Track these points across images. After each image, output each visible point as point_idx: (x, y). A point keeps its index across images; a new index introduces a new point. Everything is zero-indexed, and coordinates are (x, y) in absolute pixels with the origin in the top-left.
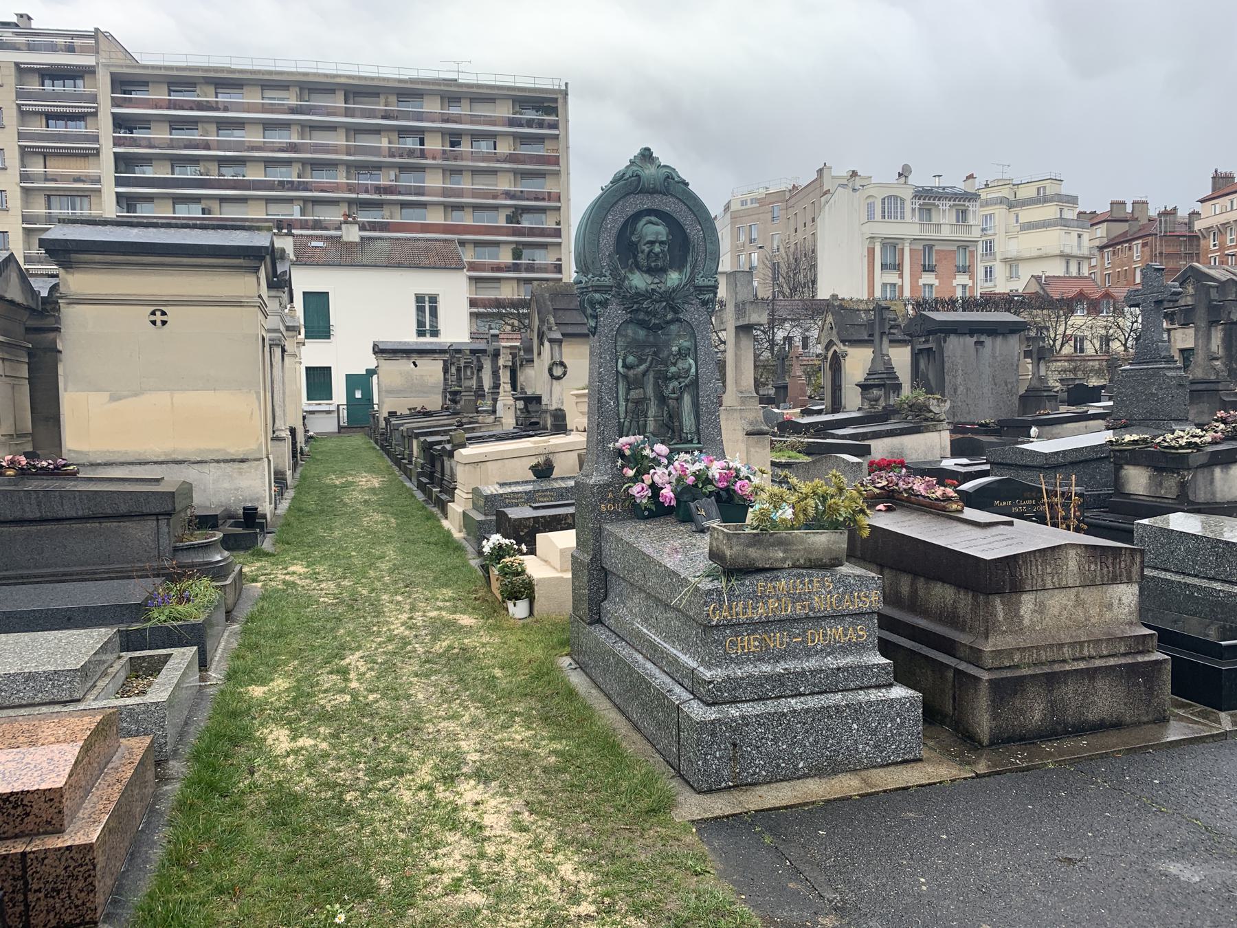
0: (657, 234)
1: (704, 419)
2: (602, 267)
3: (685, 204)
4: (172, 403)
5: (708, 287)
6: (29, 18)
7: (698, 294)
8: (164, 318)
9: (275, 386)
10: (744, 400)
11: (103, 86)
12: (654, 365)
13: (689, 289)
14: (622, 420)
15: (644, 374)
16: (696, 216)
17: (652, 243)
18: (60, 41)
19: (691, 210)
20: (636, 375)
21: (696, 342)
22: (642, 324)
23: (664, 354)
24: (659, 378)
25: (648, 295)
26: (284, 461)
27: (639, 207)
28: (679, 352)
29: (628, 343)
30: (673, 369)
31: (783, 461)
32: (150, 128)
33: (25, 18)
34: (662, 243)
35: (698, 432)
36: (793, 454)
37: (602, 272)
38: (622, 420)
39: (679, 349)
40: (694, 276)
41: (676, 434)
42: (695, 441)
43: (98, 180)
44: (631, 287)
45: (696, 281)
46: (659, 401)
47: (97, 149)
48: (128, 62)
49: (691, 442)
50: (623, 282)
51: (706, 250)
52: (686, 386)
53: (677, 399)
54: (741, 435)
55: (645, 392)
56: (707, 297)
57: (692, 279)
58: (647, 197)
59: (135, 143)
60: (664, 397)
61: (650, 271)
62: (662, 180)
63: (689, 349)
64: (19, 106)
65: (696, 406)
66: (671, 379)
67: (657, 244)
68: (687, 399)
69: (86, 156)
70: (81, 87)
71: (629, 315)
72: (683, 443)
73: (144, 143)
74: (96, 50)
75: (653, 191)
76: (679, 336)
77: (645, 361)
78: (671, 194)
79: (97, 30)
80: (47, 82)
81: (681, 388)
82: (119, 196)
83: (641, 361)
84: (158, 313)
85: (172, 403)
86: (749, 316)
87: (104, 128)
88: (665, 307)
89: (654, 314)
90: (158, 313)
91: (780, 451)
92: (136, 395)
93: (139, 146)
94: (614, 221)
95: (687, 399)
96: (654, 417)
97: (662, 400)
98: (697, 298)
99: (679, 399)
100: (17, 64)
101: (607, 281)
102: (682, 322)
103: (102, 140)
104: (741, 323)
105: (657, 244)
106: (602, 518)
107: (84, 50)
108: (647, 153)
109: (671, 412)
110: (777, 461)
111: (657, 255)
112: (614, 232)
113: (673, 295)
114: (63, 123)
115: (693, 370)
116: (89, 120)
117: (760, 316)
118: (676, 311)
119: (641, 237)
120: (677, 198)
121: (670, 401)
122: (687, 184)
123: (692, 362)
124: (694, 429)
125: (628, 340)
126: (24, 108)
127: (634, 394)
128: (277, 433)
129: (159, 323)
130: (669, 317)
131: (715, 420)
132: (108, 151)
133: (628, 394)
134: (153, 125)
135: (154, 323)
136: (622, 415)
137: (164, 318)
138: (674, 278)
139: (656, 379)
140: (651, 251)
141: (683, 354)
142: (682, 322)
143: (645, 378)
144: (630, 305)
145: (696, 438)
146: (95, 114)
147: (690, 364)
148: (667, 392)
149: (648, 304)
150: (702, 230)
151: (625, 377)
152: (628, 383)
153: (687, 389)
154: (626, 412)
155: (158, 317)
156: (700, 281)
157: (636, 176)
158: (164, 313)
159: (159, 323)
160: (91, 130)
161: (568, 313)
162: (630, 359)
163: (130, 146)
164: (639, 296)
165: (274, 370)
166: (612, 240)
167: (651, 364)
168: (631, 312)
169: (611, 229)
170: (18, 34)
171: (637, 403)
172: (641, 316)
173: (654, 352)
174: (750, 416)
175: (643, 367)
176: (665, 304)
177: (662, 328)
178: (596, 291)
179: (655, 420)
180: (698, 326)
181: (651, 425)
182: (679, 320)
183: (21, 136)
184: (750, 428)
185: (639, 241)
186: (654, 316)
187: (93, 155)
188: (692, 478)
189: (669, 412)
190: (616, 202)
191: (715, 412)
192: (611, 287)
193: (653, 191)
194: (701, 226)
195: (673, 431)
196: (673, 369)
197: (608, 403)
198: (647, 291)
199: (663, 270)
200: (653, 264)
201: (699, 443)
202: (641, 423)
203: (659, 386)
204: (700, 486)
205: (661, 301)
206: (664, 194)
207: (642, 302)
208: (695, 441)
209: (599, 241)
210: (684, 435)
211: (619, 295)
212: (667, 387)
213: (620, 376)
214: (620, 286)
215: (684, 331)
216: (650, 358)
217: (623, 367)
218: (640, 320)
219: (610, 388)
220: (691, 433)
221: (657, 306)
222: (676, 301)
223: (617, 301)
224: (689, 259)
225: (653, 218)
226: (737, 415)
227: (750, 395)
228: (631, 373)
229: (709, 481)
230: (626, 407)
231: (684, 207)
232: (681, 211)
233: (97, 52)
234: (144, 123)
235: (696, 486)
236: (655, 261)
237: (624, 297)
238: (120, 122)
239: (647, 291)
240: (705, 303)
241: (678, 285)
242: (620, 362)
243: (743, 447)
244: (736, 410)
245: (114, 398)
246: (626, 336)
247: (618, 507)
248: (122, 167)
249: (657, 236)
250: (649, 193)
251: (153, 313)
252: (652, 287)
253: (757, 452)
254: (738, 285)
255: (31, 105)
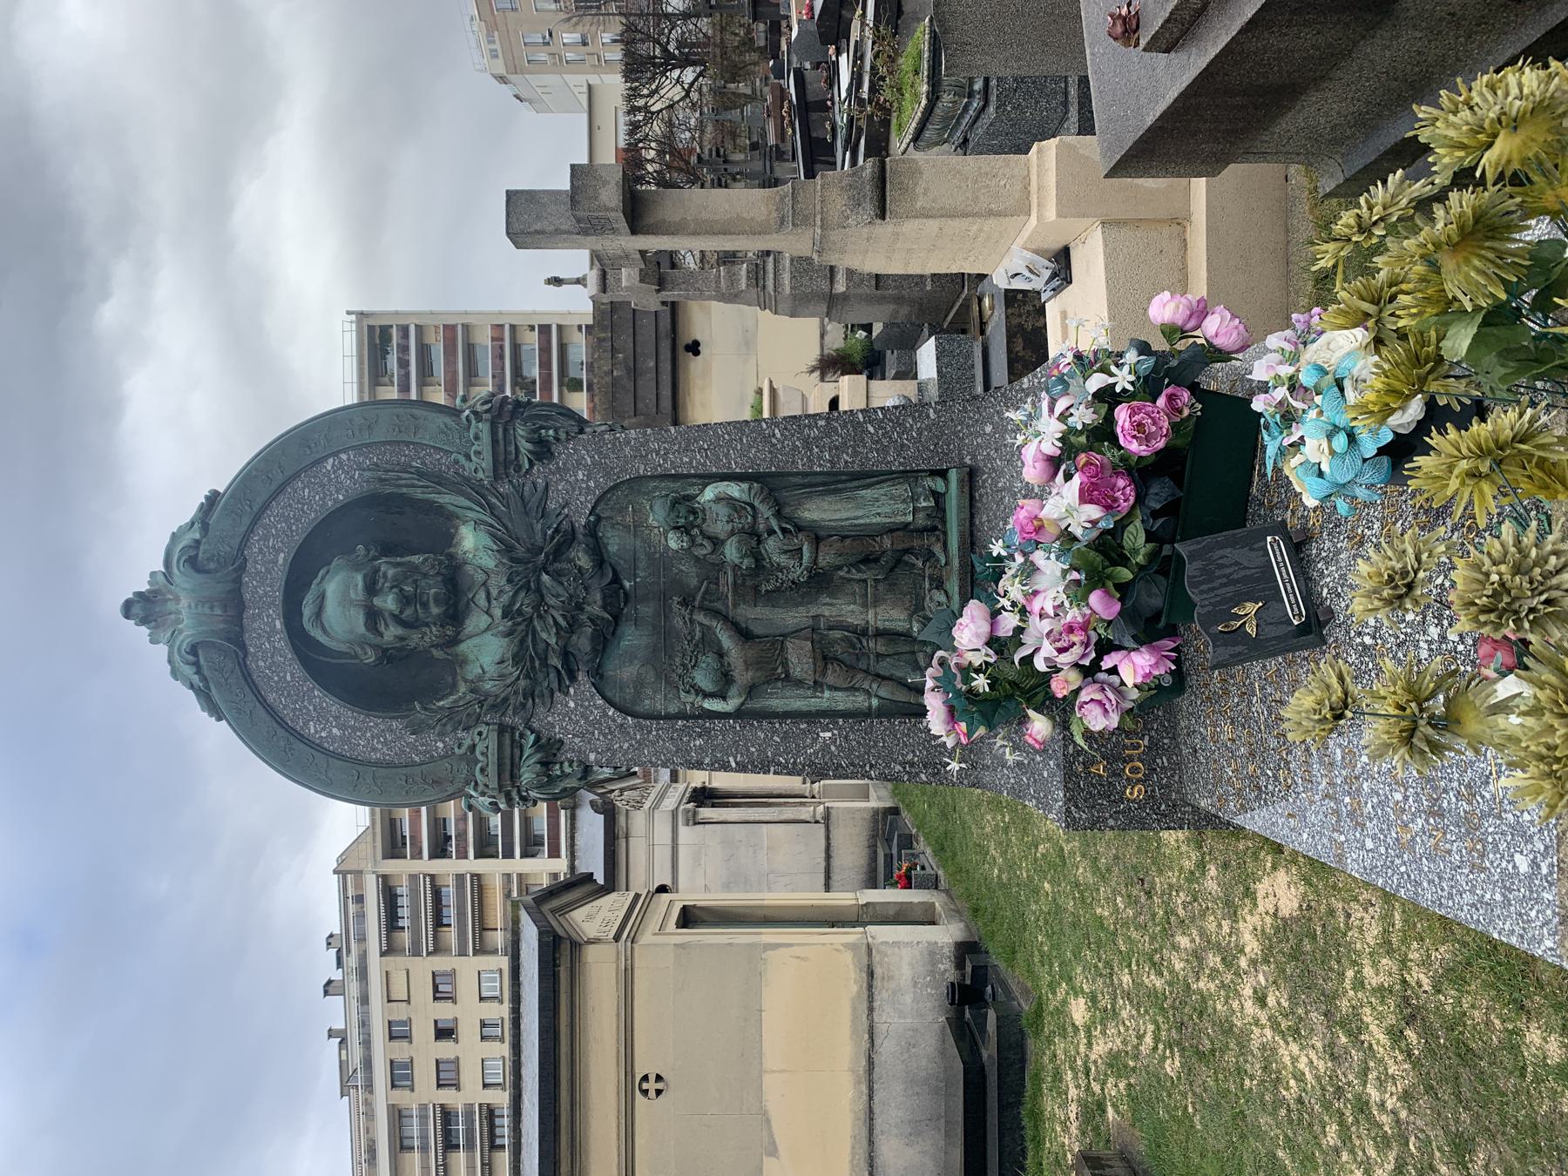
0: (345, 601)
1: (873, 460)
2: (448, 755)
3: (266, 506)
4: (781, 1071)
5: (495, 442)
6: (331, 936)
7: (519, 468)
8: (652, 1078)
9: (752, 819)
10: (797, 218)
11: (400, 868)
12: (718, 605)
13: (502, 497)
14: (875, 702)
15: (744, 634)
16: (296, 476)
17: (373, 617)
18: (352, 908)
19: (280, 490)
20: (747, 666)
21: (653, 477)
22: (604, 640)
23: (689, 573)
24: (756, 589)
25: (520, 626)
26: (859, 810)
27: (281, 642)
28: (684, 530)
29: (658, 676)
30: (731, 552)
31: (925, 88)
32: (444, 819)
33: (331, 940)
34: (371, 589)
35: (909, 475)
36: (905, 63)
37: (462, 757)
38: (875, 702)
39: (677, 528)
40: (467, 480)
41: (916, 543)
42: (939, 485)
43: (507, 877)
44: (502, 676)
45: (480, 475)
46: (820, 591)
47: (472, 875)
48: (369, 839)
49: (938, 497)
50: (487, 695)
51: (389, 443)
52: (778, 514)
53: (817, 540)
54: (885, 229)
55: (796, 633)
56: (525, 446)
57: (477, 492)
58: (253, 618)
59: (462, 836)
60: (810, 577)
61: (455, 615)
62: (200, 578)
63: (675, 503)
64: (429, 954)
65: (836, 483)
66: (757, 557)
67: (377, 601)
68: (818, 511)
69: (481, 887)
70: (403, 890)
71: (581, 676)
72: (944, 521)
73: (461, 826)
74: (359, 873)
75: (234, 604)
76: (638, 527)
77: (706, 630)
78: (241, 549)
79: (335, 872)
80: (400, 924)
81: (784, 531)
82: (524, 855)
83: (708, 643)
84: (645, 1086)
85: (781, 1071)
86: (607, 209)
87: (447, 868)
88: (557, 576)
89: (575, 607)
90: (645, 1086)
91: (899, 90)
92: (768, 1121)
93: (465, 832)
94: (322, 715)
95: (818, 511)
96: (865, 605)
97: (819, 582)
98: (528, 472)
99: (818, 536)
100: (383, 954)
101: (487, 743)
102: (599, 519)
103: (461, 871)
104: (623, 224)
105: (377, 601)
106: (1165, 798)
107: (359, 885)
108: (136, 609)
109: (852, 560)
110: (924, 102)
111: (405, 600)
112: (351, 716)
113: (521, 551)
114: (445, 910)
115: (735, 490)
116: (439, 882)
117: (605, 183)
118: (569, 538)
119: (363, 643)
120: (251, 529)
121: (822, 562)
122: (213, 498)
123: (709, 493)
124: (902, 490)
125: (651, 677)
126: (431, 949)
127: (799, 659)
128: (819, 817)
129: (660, 1086)
130: (584, 561)
131: (879, 425)
132: (472, 865)
133: (799, 683)
134: (441, 816)
135: (659, 1092)
136: (859, 701)
137: (652, 1078)
138: (471, 541)
139: (757, 596)
140: (398, 620)
141: (687, 516)
142: (599, 519)
143: (758, 630)
144: (553, 675)
145: (929, 482)
146: (433, 877)
147: (718, 500)
148: (798, 573)
149: (546, 629)
150: (335, 454)
151: (751, 691)
152: (771, 679)
153: (787, 510)
154: (853, 689)
155: (651, 1086)
156: (481, 464)
157: (195, 654)
158: (645, 1078)
159: (660, 1086)
160: (451, 881)
161: (640, 392)
162: (703, 679)
163: (466, 840)
164: (526, 655)
165: (730, 820)
166: (375, 723)
167: (716, 614)
168: (573, 678)
169: (342, 727)
170: (349, 951)
171: (825, 658)
172: (582, 642)
173: (685, 603)
174: (838, 202)
175: (726, 640)
176: (545, 577)
177: (616, 579)
178: (514, 777)
179: (877, 602)
180: (607, 475)
181: (891, 616)
182: (592, 530)
183: (462, 953)
184: (869, 208)
185: (375, 647)
186: (579, 607)
187: (479, 880)
188: (1095, 598)
189: (852, 565)
190: (271, 710)
191: (858, 425)
192: (502, 729)
193: (234, 604)
194: (325, 458)
195: (907, 551)
196: (731, 552)
197: (825, 748)
198: (509, 634)
199: (453, 577)
200: (435, 610)
201: (943, 474)
202: (881, 649)
203: (777, 590)
204: (1126, 574)
205: (538, 590)
206: (242, 568)
207: (541, 646)
208: (939, 485)
209: (378, 764)
210: (921, 520)
211: (523, 705)
212: (780, 568)
213: (749, 705)
214: (500, 705)
215: (622, 510)
216: (700, 617)
217: (724, 698)
218: (594, 649)
219: (785, 737)
220: (914, 499)
221: (552, 601)
222: (539, 537)
223: (540, 710)
224: (419, 494)
225: (307, 611)
226: (835, 236)
227: (788, 200)
228: (742, 676)
229: (1108, 546)
230: (836, 689)
231: (275, 508)
232: (287, 520)
233: (361, 872)
234: (438, 825)
235: (1123, 589)
236: (425, 605)
237: (530, 694)
238: (440, 850)
239: (509, 634)
240: (543, 451)
241: (493, 535)
242: (709, 705)
243: (910, 227)
244: (823, 237)
245: (773, 1151)
246: (639, 684)
247: (1137, 747)
248: (491, 850)
249: (351, 602)
250: (240, 617)
251: (645, 1092)
252: (498, 613)
253: (926, 190)
254: (538, 227)
255: (426, 941)
